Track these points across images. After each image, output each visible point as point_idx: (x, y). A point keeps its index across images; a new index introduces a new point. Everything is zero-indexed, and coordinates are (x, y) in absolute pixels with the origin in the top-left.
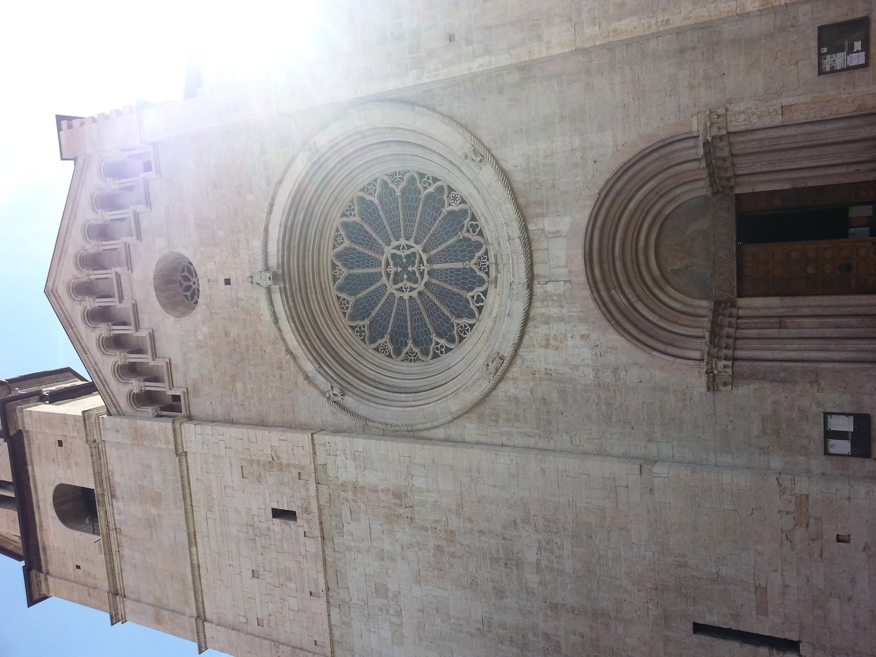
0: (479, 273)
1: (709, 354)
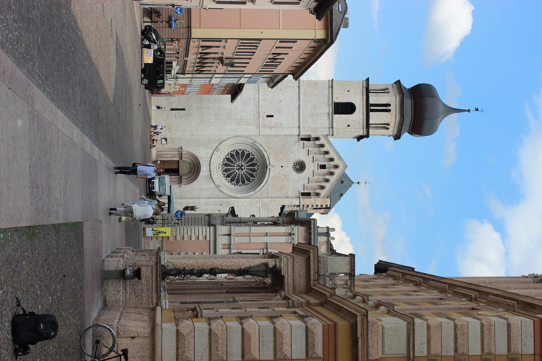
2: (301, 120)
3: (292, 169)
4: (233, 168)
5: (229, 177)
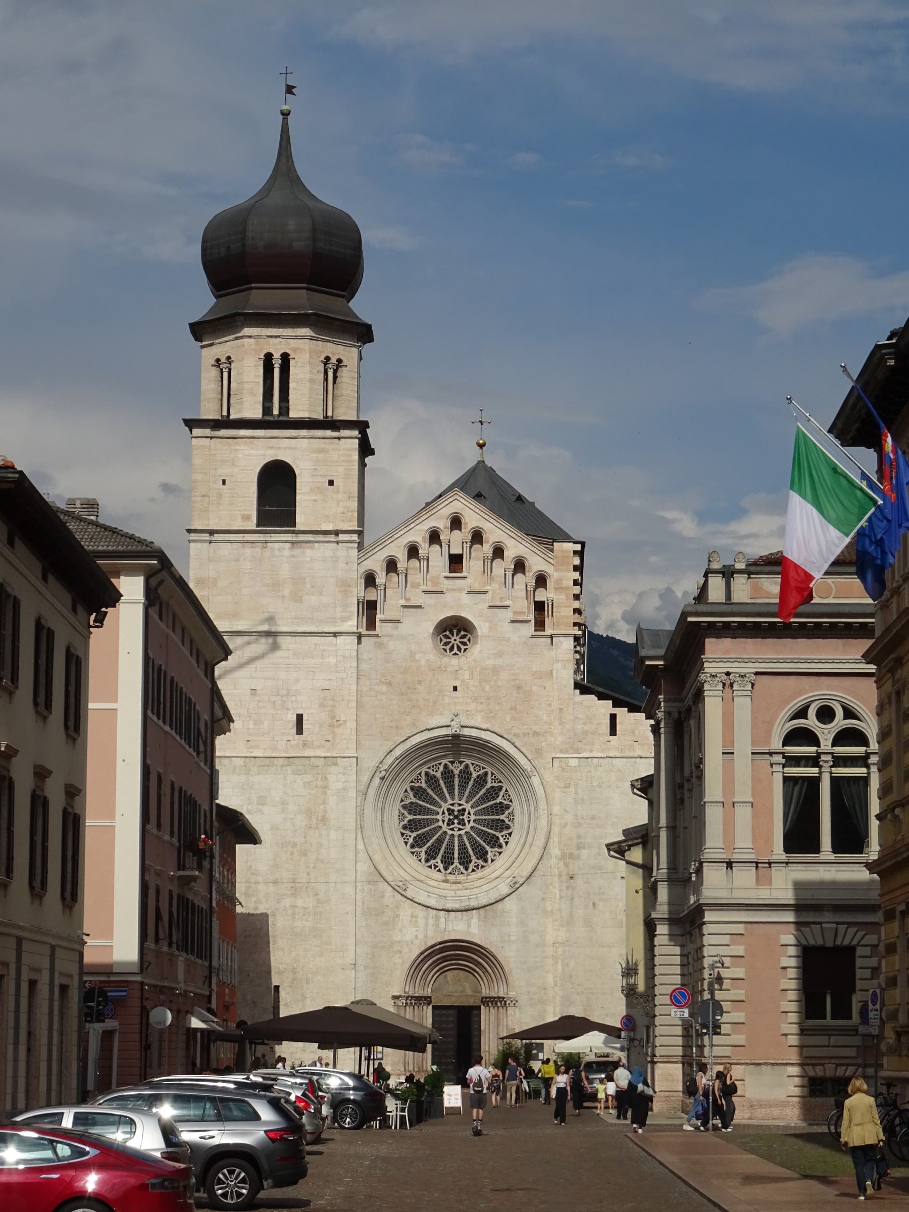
0: (451, 867)
1: (409, 996)
2: (313, 629)
3: (463, 659)
4: (456, 839)
5: (487, 852)
